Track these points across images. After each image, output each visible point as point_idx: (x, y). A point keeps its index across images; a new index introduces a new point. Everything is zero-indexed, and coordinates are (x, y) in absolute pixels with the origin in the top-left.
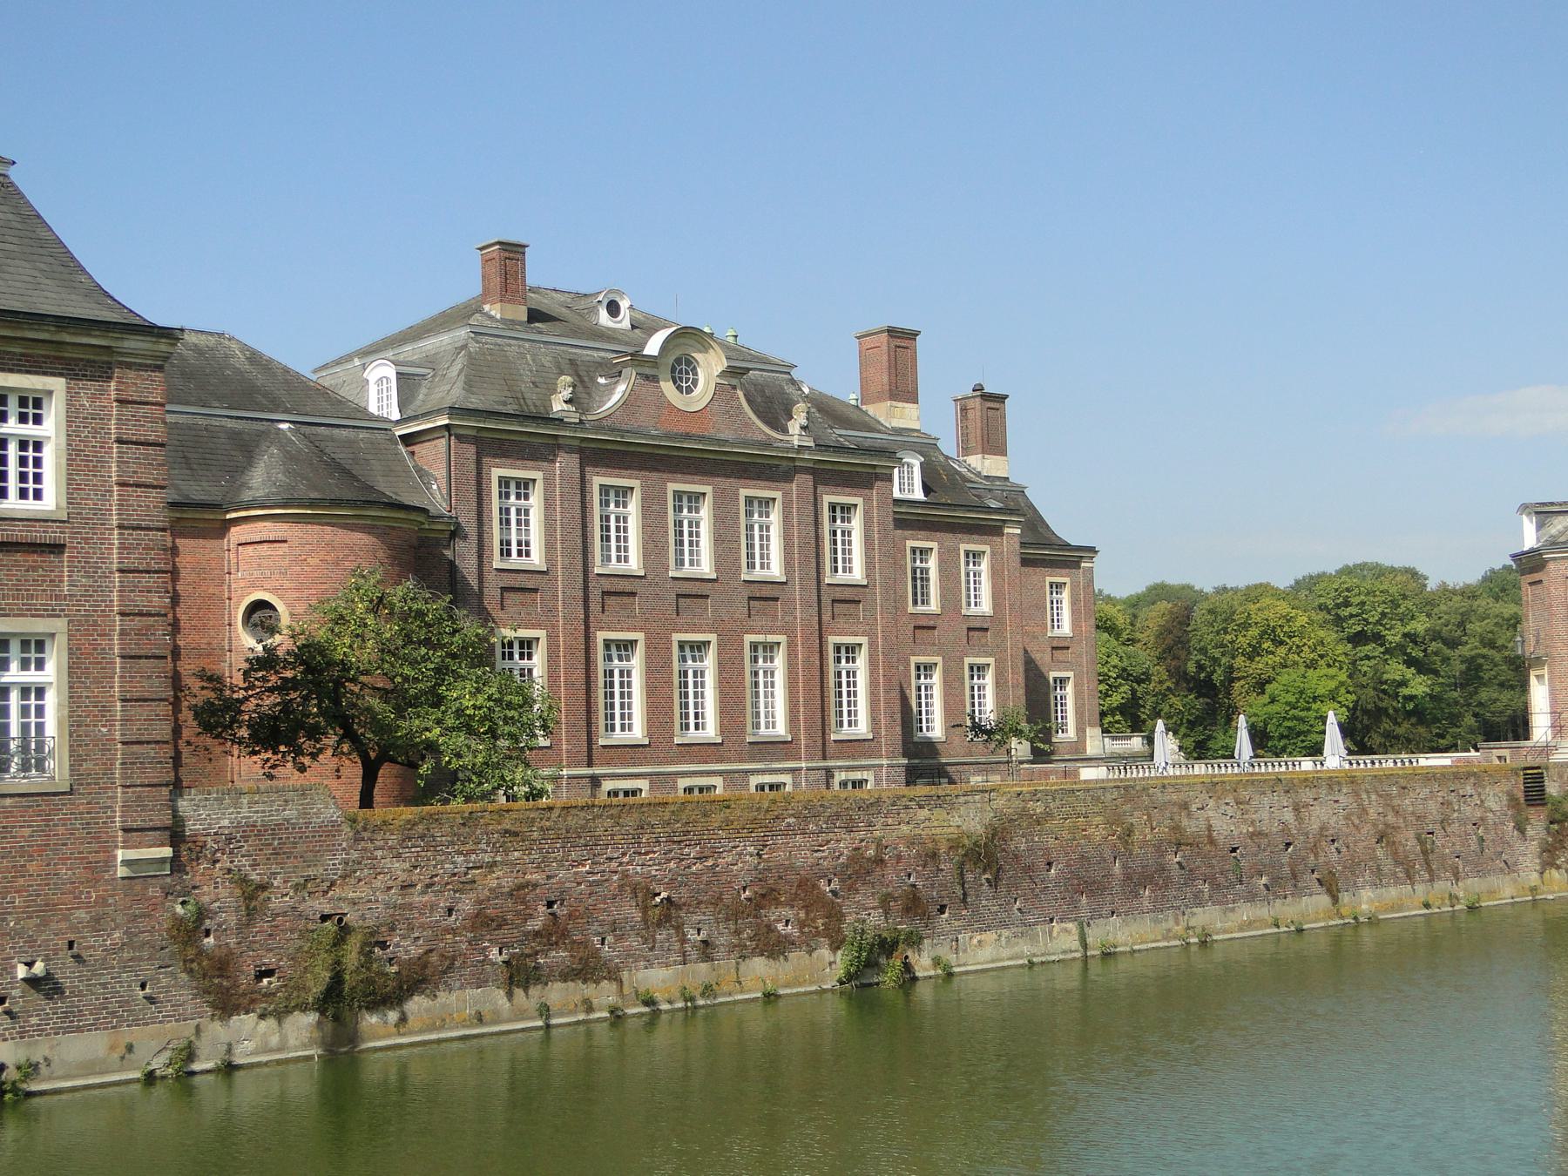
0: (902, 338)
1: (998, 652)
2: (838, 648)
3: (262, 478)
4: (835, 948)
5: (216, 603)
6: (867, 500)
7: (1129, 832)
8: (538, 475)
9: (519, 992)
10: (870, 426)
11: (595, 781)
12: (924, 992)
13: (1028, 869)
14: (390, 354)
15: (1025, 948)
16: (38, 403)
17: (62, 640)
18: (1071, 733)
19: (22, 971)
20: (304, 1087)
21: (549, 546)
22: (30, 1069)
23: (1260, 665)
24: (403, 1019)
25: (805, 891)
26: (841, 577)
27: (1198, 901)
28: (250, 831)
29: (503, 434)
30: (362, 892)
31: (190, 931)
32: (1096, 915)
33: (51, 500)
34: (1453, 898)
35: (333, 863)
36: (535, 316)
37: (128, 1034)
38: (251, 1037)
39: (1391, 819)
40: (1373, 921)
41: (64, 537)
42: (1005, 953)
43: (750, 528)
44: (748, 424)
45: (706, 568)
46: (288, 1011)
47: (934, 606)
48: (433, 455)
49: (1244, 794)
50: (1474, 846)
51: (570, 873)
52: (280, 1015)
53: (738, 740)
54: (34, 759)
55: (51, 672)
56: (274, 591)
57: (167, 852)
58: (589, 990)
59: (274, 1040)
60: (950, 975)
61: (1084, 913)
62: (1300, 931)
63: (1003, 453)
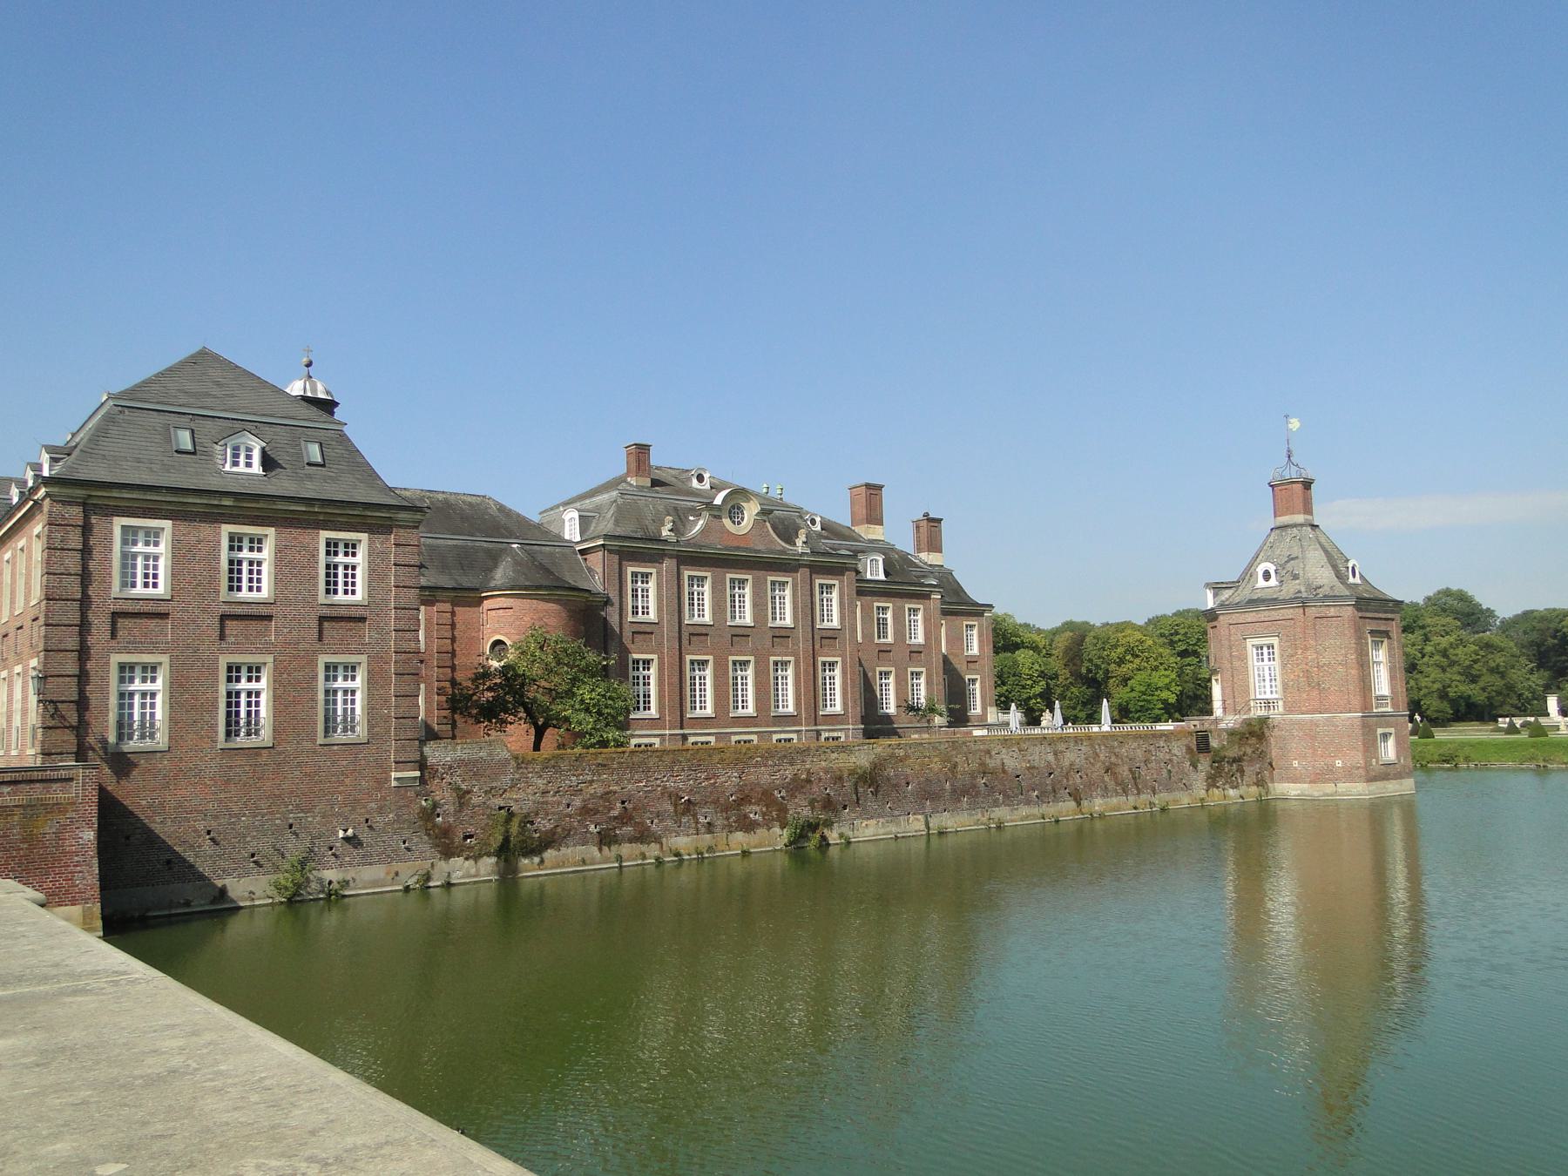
0: (874, 490)
2: (824, 664)
3: (501, 575)
4: (782, 828)
5: (475, 641)
6: (841, 582)
7: (955, 766)
8: (654, 571)
9: (605, 848)
10: (857, 538)
11: (685, 737)
12: (834, 852)
14: (578, 505)
15: (893, 829)
16: (354, 546)
17: (364, 665)
18: (979, 710)
19: (341, 834)
20: (488, 895)
21: (659, 610)
22: (345, 884)
23: (1124, 669)
24: (542, 861)
25: (766, 797)
26: (826, 625)
27: (996, 804)
28: (462, 763)
29: (634, 549)
31: (429, 814)
32: (935, 811)
33: (360, 596)
34: (1152, 804)
35: (506, 780)
36: (656, 483)
37: (396, 866)
38: (460, 869)
40: (1102, 816)
41: (366, 613)
42: (882, 831)
43: (774, 598)
44: (772, 541)
45: (748, 620)
46: (480, 856)
47: (890, 639)
48: (596, 560)
49: (1025, 746)
50: (1165, 772)
51: (634, 786)
52: (476, 858)
53: (766, 714)
54: (349, 726)
55: (359, 683)
56: (505, 635)
57: (418, 774)
58: (644, 848)
59: (473, 871)
60: (849, 843)
61: (928, 810)
62: (1057, 821)
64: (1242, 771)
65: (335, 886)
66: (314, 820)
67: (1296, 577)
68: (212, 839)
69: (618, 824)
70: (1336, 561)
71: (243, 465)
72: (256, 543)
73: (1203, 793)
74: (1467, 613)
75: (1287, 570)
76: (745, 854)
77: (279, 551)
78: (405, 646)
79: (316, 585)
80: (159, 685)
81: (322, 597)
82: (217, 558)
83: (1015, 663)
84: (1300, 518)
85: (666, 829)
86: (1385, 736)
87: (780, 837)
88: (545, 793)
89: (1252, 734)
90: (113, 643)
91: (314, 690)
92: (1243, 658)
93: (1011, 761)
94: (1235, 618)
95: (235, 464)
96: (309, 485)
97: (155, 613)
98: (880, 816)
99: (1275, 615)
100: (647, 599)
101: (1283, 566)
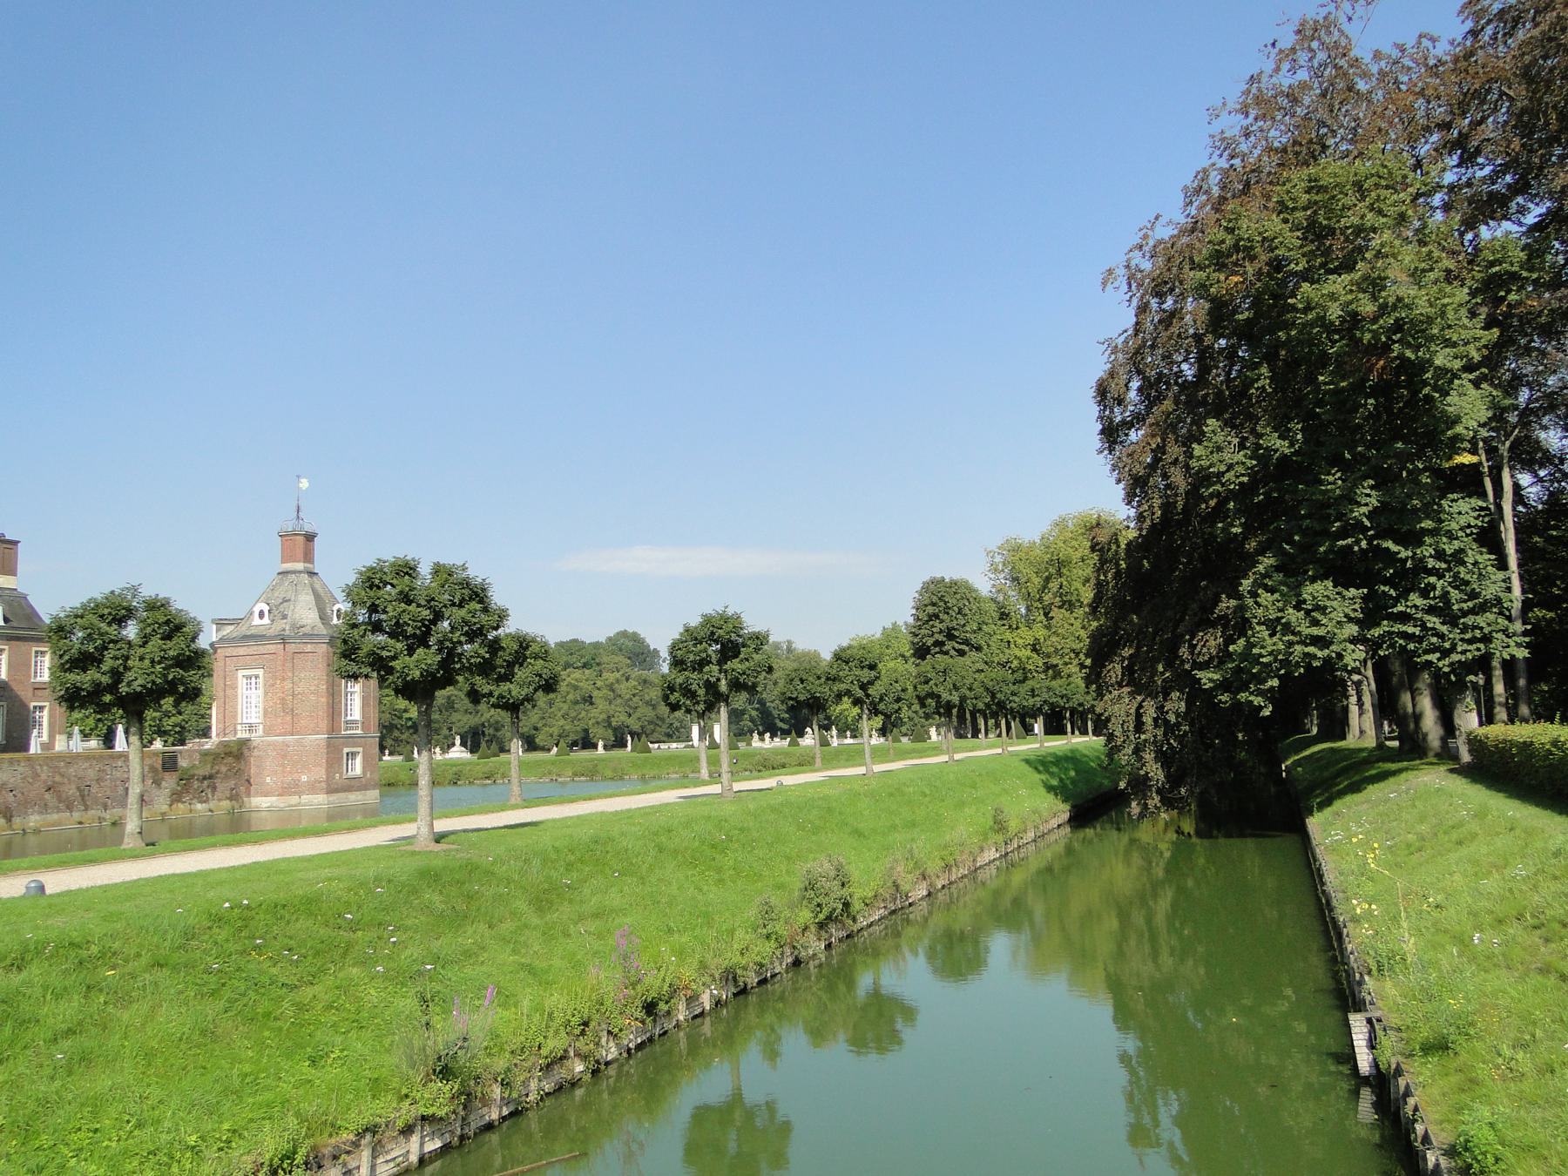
39: (58, 778)
40: (37, 831)
63: (14, 574)
64: (214, 788)
67: (285, 617)
73: (165, 808)
75: (278, 610)
84: (300, 566)
86: (353, 755)
89: (229, 754)
92: (235, 688)
94: (229, 652)
99: (262, 649)
101: (277, 607)
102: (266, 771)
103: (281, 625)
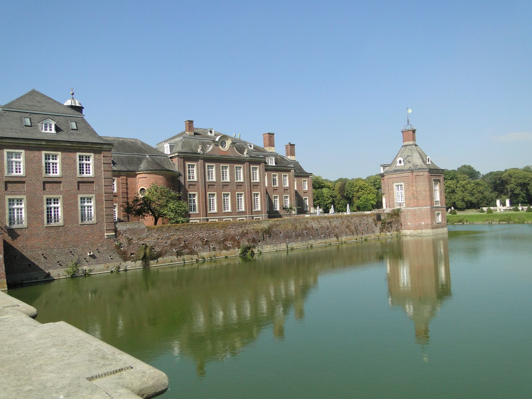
0: (271, 135)
1: (290, 194)
2: (254, 194)
3: (143, 166)
4: (239, 248)
5: (135, 188)
7: (296, 227)
8: (195, 164)
9: (179, 257)
10: (265, 151)
11: (207, 220)
12: (256, 257)
13: (276, 234)
14: (169, 142)
15: (276, 248)
17: (94, 198)
19: (89, 254)
23: (359, 194)
25: (233, 239)
26: (255, 181)
27: (310, 239)
28: (129, 230)
29: (188, 157)
30: (150, 240)
31: (119, 247)
33: (92, 174)
34: (362, 238)
35: (144, 235)
36: (196, 134)
37: (108, 264)
38: (130, 265)
39: (349, 224)
40: (345, 242)
44: (236, 153)
45: (228, 180)
46: (137, 260)
47: (277, 185)
48: (176, 160)
49: (319, 220)
50: (366, 228)
51: (188, 236)
52: (135, 261)
53: (235, 211)
55: (92, 204)
56: (145, 186)
57: (114, 234)
58: (192, 256)
59: (134, 265)
60: (261, 253)
61: (287, 242)
64: (392, 227)
65: (87, 271)
66: (79, 250)
67: (410, 162)
68: (44, 257)
69: (183, 249)
70: (422, 156)
71: (49, 131)
72: (55, 157)
73: (379, 234)
74: (472, 173)
75: (407, 160)
76: (226, 257)
77: (63, 159)
78: (108, 191)
79: (76, 171)
80: (23, 206)
81: (78, 175)
82: (41, 162)
83: (322, 193)
84: (411, 143)
85: (200, 250)
86: (438, 214)
87: (238, 251)
88: (158, 239)
89: (395, 214)
90: (6, 192)
91: (77, 206)
92: (392, 190)
93: (315, 225)
94: (389, 176)
95: (46, 130)
96: (72, 137)
97: (20, 181)
98: (271, 244)
99: (403, 175)
100: (194, 173)
101: (406, 159)
102: (408, 220)
103: (408, 166)
